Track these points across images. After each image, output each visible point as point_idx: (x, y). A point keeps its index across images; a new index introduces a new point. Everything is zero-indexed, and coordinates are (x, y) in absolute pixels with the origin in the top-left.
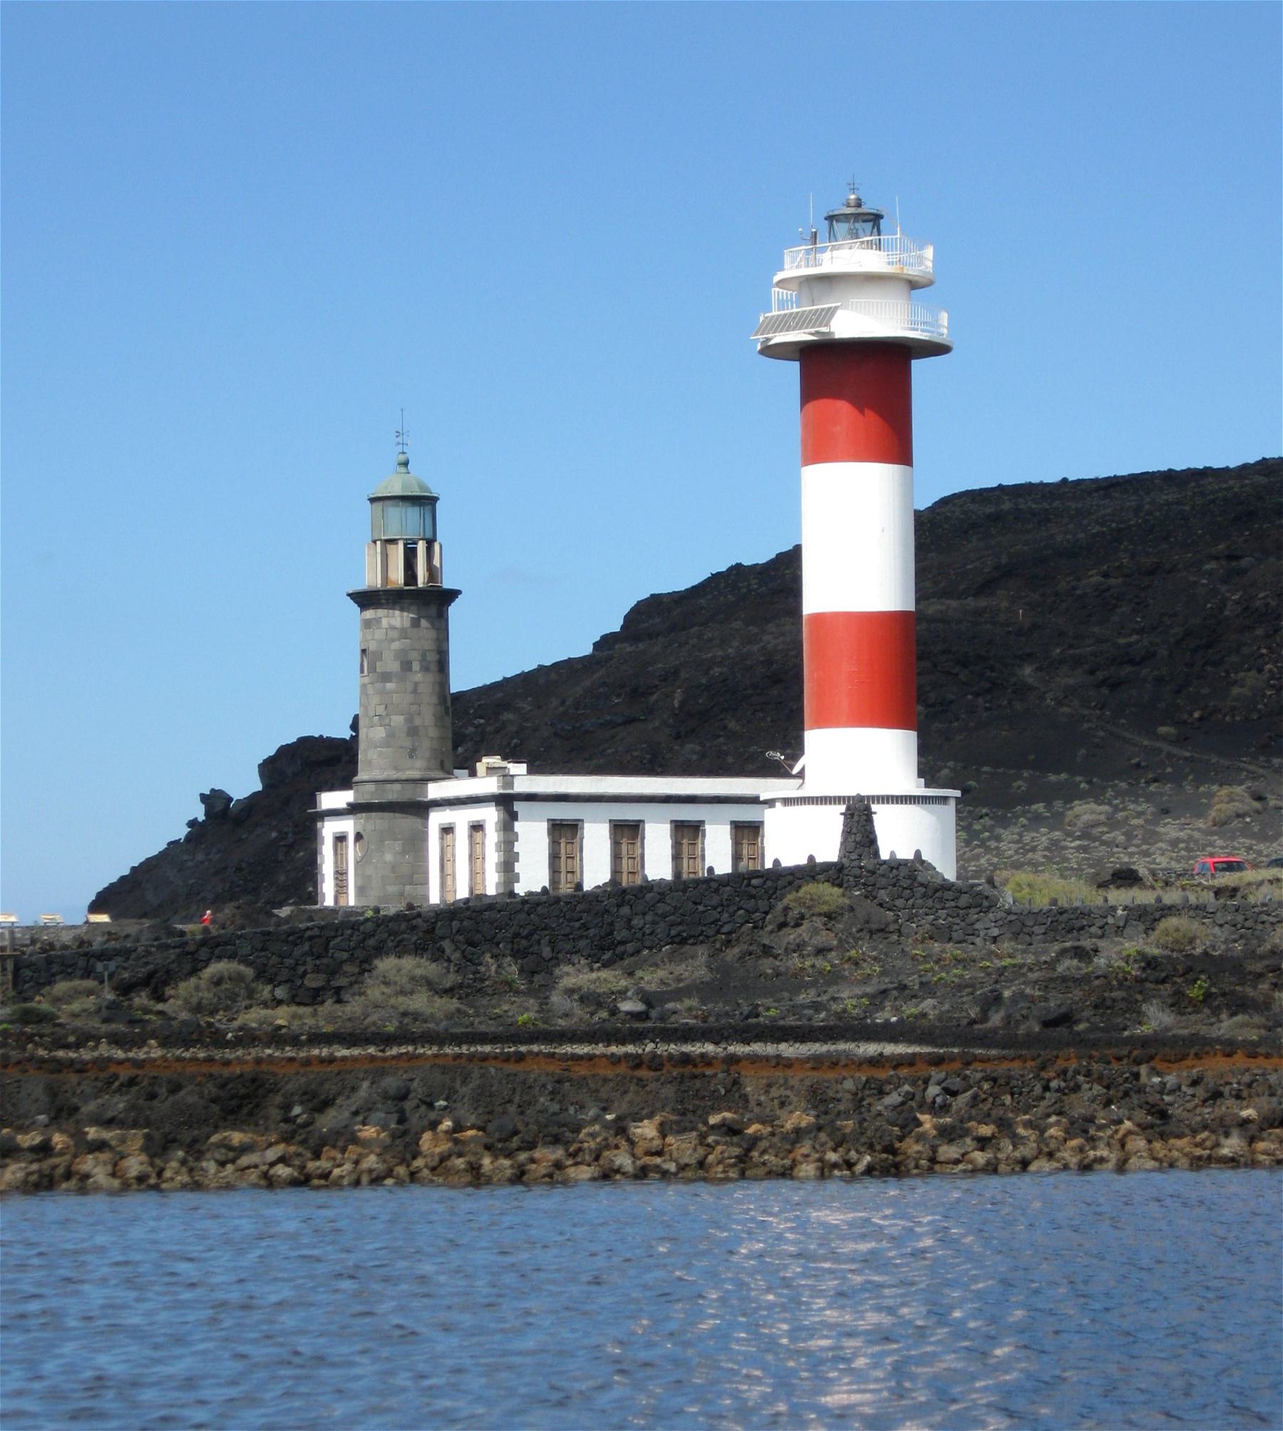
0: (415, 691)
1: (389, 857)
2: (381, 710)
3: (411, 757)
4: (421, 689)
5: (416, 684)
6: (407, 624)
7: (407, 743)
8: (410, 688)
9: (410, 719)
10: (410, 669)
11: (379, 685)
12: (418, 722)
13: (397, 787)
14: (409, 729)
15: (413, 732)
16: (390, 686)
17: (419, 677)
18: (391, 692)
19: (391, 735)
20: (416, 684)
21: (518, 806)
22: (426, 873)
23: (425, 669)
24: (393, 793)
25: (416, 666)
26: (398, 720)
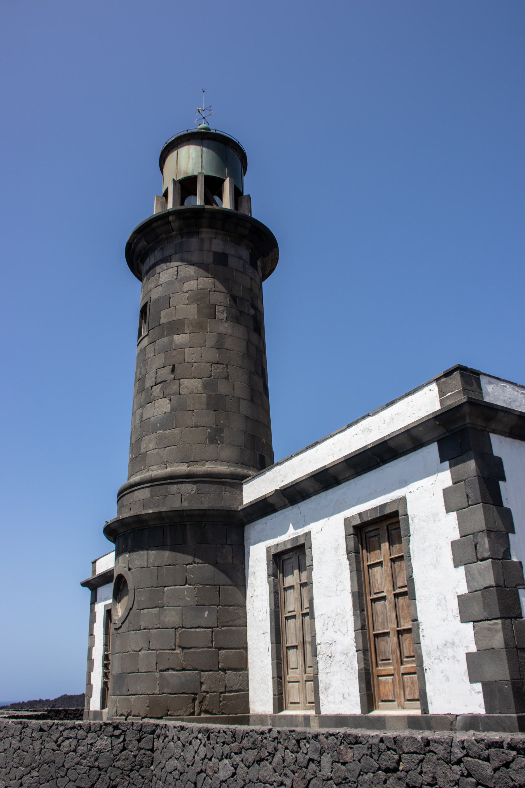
0: (219, 346)
1: (172, 617)
2: (165, 373)
3: (213, 440)
4: (228, 343)
5: (221, 336)
6: (209, 259)
7: (208, 419)
8: (211, 340)
9: (210, 385)
10: (213, 316)
11: (165, 340)
12: (223, 388)
13: (189, 488)
14: (209, 397)
15: (215, 403)
16: (178, 339)
17: (225, 327)
18: (182, 348)
19: (180, 408)
20: (221, 336)
21: (501, 446)
22: (243, 647)
23: (236, 318)
24: (181, 499)
25: (222, 314)
26: (191, 385)
